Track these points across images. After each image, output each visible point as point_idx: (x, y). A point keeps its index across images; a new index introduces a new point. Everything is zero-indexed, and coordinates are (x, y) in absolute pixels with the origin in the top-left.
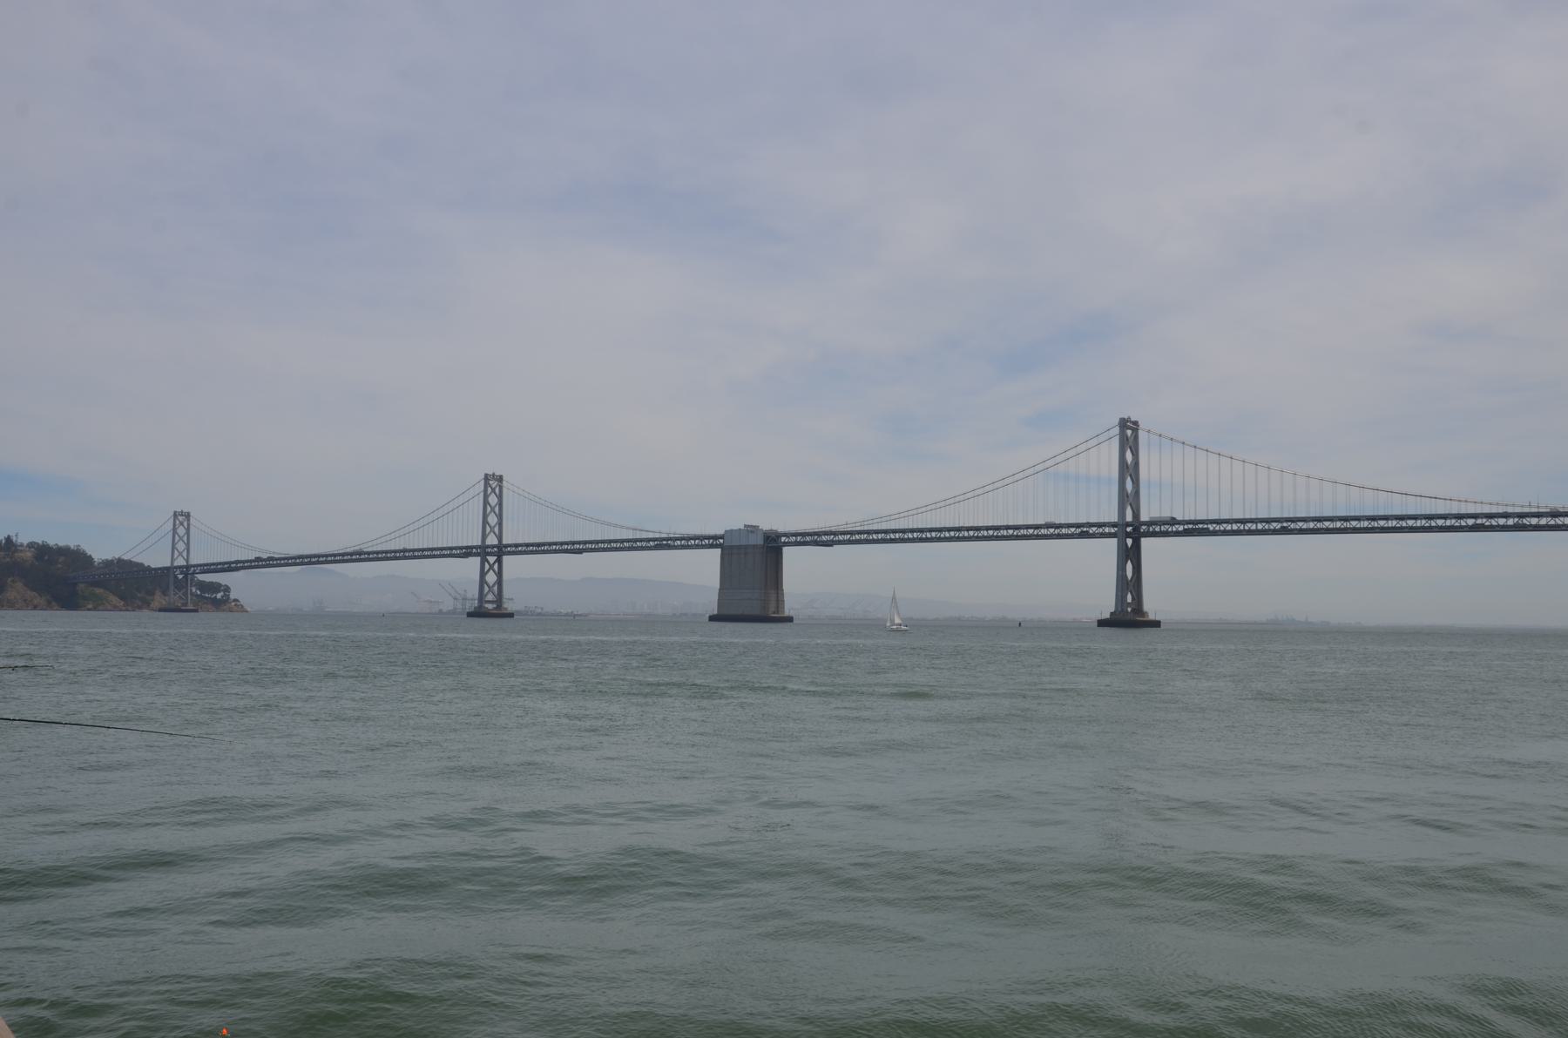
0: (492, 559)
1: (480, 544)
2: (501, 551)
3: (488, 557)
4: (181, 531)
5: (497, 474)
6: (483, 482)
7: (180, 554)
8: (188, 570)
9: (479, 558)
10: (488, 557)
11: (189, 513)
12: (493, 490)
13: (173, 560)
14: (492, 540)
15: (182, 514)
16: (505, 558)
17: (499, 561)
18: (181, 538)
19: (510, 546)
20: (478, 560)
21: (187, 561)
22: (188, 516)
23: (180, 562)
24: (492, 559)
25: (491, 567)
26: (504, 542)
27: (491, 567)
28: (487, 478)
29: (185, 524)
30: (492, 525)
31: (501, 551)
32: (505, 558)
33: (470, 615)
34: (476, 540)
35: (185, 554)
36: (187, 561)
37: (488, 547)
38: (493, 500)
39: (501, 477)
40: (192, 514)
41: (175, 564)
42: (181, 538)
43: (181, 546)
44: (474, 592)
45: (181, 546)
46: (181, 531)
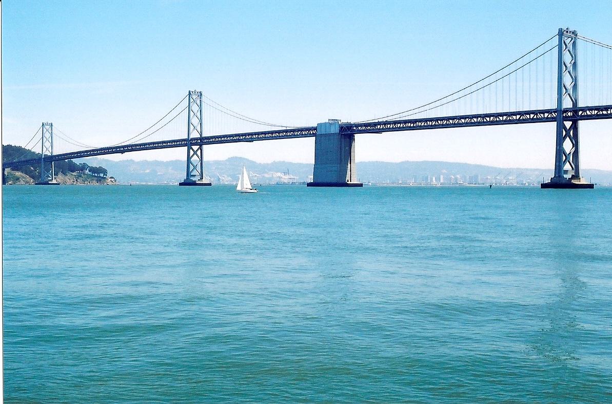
0: (568, 124)
1: (554, 106)
2: (577, 115)
3: (564, 122)
5: (571, 29)
6: (558, 36)
8: (202, 141)
14: (567, 104)
16: (581, 124)
17: (575, 127)
20: (553, 125)
21: (201, 135)
23: (195, 135)
24: (568, 124)
25: (568, 131)
26: (581, 104)
27: (568, 135)
28: (561, 33)
29: (198, 102)
31: (577, 115)
32: (581, 124)
33: (544, 186)
36: (201, 135)
37: (566, 111)
38: (567, 58)
41: (191, 137)
43: (195, 121)
44: (551, 164)
45: (195, 121)
46: (195, 108)
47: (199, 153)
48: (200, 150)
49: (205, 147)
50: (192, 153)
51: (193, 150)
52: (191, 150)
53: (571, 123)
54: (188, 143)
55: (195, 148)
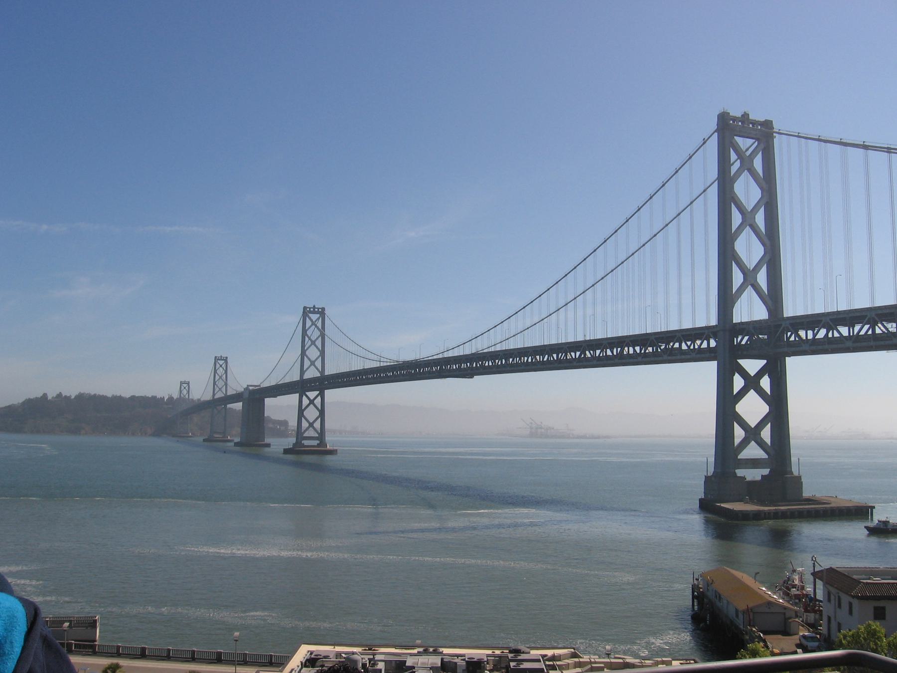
0: (752, 366)
1: (713, 322)
3: (744, 363)
4: (314, 333)
5: (757, 115)
7: (313, 363)
9: (713, 365)
10: (744, 363)
11: (323, 309)
12: (747, 164)
13: (302, 372)
15: (314, 310)
16: (795, 365)
18: (313, 343)
19: (812, 321)
22: (322, 312)
23: (312, 373)
29: (319, 324)
30: (751, 264)
32: (795, 365)
34: (708, 317)
35: (318, 364)
39: (768, 124)
40: (326, 312)
41: (307, 376)
42: (313, 343)
43: (313, 353)
45: (313, 353)
46: (314, 333)
47: (318, 401)
48: (319, 398)
49: (327, 392)
50: (305, 401)
51: (307, 396)
52: (304, 397)
53: (764, 362)
54: (300, 387)
55: (312, 394)
